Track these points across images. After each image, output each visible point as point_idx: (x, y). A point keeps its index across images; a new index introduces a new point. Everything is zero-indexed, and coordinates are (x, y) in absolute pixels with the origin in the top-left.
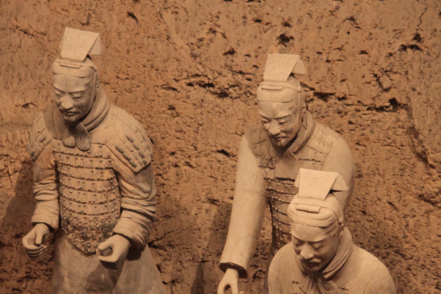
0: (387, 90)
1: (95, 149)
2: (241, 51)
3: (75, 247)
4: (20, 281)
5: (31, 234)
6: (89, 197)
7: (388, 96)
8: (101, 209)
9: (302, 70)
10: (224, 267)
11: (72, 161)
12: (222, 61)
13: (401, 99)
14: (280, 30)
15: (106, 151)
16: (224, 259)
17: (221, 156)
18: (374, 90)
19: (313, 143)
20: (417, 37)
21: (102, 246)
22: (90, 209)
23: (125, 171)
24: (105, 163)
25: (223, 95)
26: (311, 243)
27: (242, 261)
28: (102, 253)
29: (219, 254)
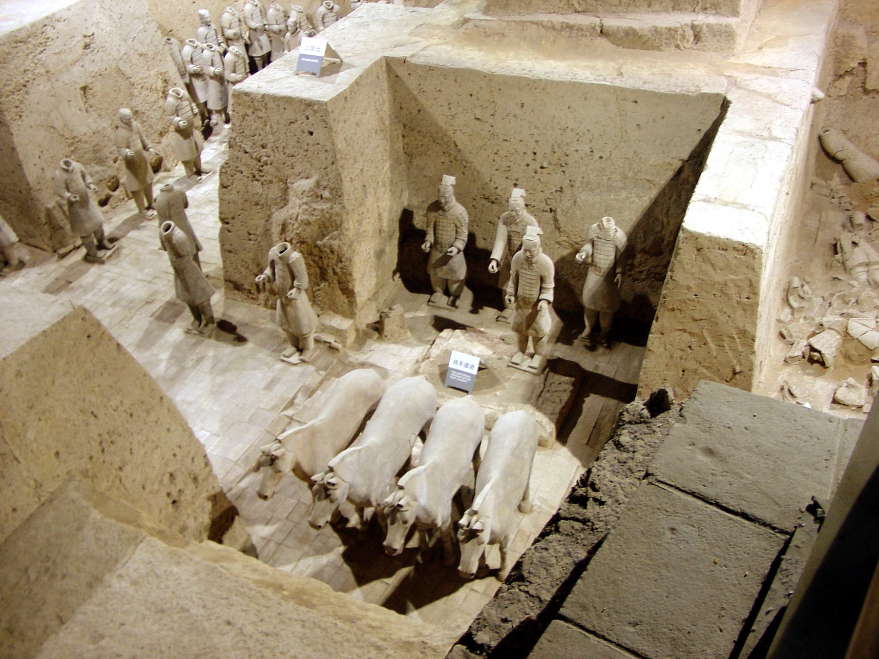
13: (554, 209)
14: (515, 182)
21: (450, 250)
27: (499, 259)
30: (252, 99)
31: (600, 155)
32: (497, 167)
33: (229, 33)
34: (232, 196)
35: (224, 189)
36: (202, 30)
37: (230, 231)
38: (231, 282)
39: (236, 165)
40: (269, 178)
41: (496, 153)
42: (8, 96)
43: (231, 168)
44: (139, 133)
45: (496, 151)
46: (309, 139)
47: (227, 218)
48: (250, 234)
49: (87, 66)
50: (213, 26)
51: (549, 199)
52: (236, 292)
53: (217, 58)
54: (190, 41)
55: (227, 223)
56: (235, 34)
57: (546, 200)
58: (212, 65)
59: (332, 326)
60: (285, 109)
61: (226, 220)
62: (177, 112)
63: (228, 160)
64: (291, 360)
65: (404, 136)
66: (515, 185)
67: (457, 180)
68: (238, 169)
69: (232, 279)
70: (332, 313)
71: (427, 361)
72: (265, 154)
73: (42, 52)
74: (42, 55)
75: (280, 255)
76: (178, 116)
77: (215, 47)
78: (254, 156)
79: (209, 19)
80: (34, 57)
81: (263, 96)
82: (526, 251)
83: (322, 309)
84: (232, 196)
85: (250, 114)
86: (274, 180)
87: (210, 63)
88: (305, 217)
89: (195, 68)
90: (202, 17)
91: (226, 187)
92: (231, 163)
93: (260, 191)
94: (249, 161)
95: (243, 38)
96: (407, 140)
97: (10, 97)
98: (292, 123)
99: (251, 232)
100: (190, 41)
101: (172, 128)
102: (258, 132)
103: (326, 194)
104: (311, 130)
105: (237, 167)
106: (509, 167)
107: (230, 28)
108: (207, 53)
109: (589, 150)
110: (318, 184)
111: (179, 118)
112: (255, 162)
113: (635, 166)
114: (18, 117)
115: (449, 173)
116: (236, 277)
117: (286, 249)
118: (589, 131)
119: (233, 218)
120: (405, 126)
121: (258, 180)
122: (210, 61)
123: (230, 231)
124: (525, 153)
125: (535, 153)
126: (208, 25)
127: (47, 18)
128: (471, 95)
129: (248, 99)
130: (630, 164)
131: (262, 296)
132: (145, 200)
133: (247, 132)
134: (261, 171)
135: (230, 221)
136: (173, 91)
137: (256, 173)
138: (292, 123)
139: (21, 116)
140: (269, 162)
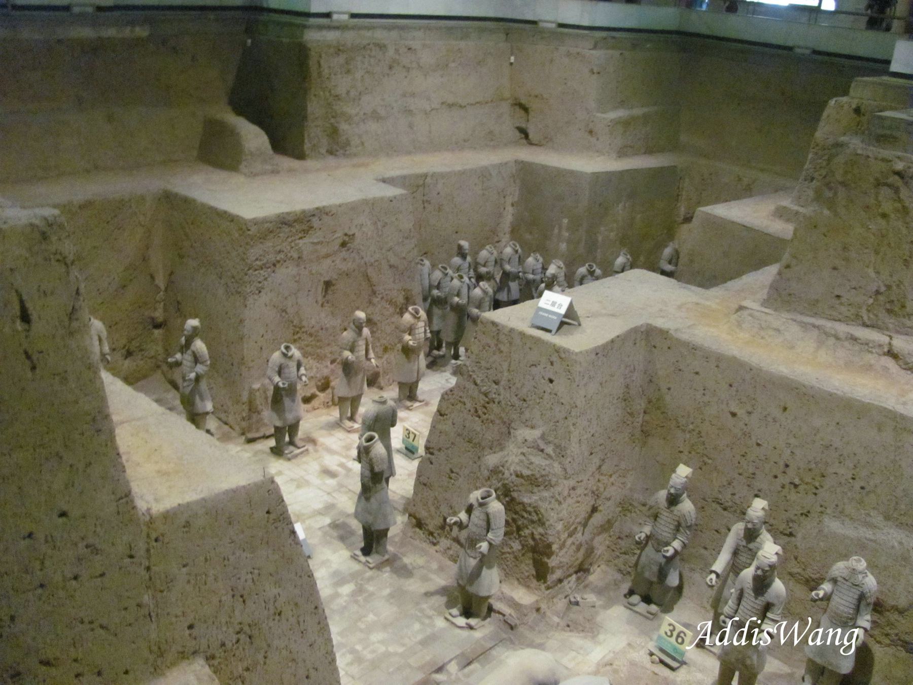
0: (790, 528)
1: (675, 512)
2: (736, 497)
3: (653, 547)
4: (621, 553)
5: (639, 535)
6: (667, 529)
7: (790, 530)
8: (669, 535)
9: (767, 508)
10: (712, 572)
11: (665, 514)
12: (730, 496)
14: (756, 492)
15: (679, 514)
16: (714, 568)
17: (716, 533)
18: (784, 526)
19: (761, 536)
20: (809, 512)
21: (666, 549)
22: (665, 534)
23: (683, 524)
24: (677, 518)
25: (725, 509)
26: (763, 570)
27: (719, 571)
28: (665, 551)
29: (711, 565)
30: (498, 330)
31: (862, 484)
32: (741, 471)
33: (483, 270)
34: (446, 426)
35: (440, 417)
36: (457, 260)
37: (431, 463)
38: (415, 518)
39: (461, 394)
40: (492, 417)
41: (744, 456)
42: (256, 270)
43: (454, 396)
44: (366, 339)
45: (743, 453)
46: (548, 387)
47: (433, 448)
48: (452, 472)
49: (338, 262)
50: (469, 259)
51: (793, 521)
52: (417, 530)
53: (465, 291)
54: (442, 267)
55: (432, 454)
56: (488, 273)
57: (788, 522)
58: (458, 295)
59: (512, 598)
60: (530, 348)
61: (431, 450)
62: (411, 330)
63: (453, 388)
64: (455, 620)
65: (645, 412)
66: (757, 496)
67: (693, 473)
68: (462, 400)
69: (417, 515)
70: (516, 582)
71: (608, 668)
72: (495, 391)
73: (301, 238)
74: (301, 241)
75: (481, 501)
76: (410, 334)
77: (466, 279)
78: (482, 390)
79: (467, 251)
80: (292, 241)
81: (512, 330)
82: (758, 568)
83: (507, 575)
84: (446, 426)
85: (492, 345)
86: (497, 422)
87: (456, 293)
88: (518, 468)
89: (439, 294)
90: (460, 247)
91: (441, 415)
92: (455, 392)
93: (478, 429)
94: (476, 392)
95: (494, 279)
96: (647, 417)
97: (257, 272)
98: (533, 365)
99: (454, 470)
100: (442, 267)
101: (399, 346)
102: (494, 366)
103: (549, 450)
104: (553, 378)
105: (461, 397)
106: (754, 474)
107: (484, 266)
108: (456, 282)
109: (851, 476)
110: (543, 437)
111: (410, 337)
112: (482, 397)
113: (903, 507)
114: (257, 292)
115: (687, 464)
116: (423, 514)
117: (489, 496)
118: (855, 454)
119: (440, 450)
120: (650, 402)
121: (480, 417)
122: (457, 291)
123: (431, 463)
124: (775, 463)
125: (787, 466)
126: (463, 256)
127: (317, 208)
128: (731, 386)
129: (494, 329)
130: (897, 503)
131: (445, 543)
132: (349, 410)
133: (483, 363)
134: (485, 408)
135: (436, 452)
136: (413, 309)
137: (478, 408)
138: (533, 365)
139: (260, 292)
140: (496, 401)
